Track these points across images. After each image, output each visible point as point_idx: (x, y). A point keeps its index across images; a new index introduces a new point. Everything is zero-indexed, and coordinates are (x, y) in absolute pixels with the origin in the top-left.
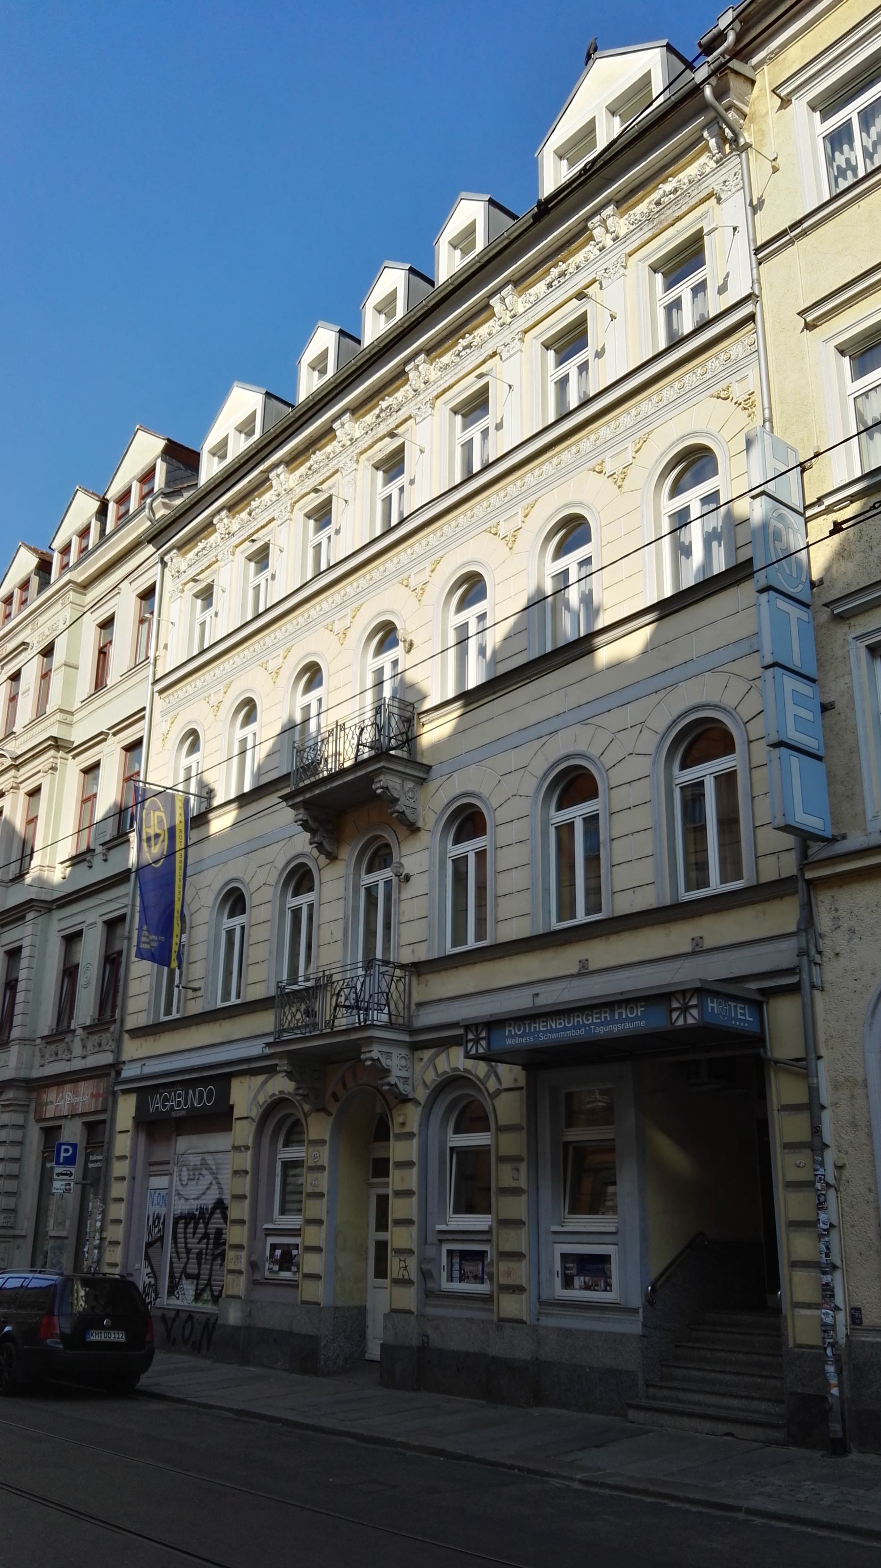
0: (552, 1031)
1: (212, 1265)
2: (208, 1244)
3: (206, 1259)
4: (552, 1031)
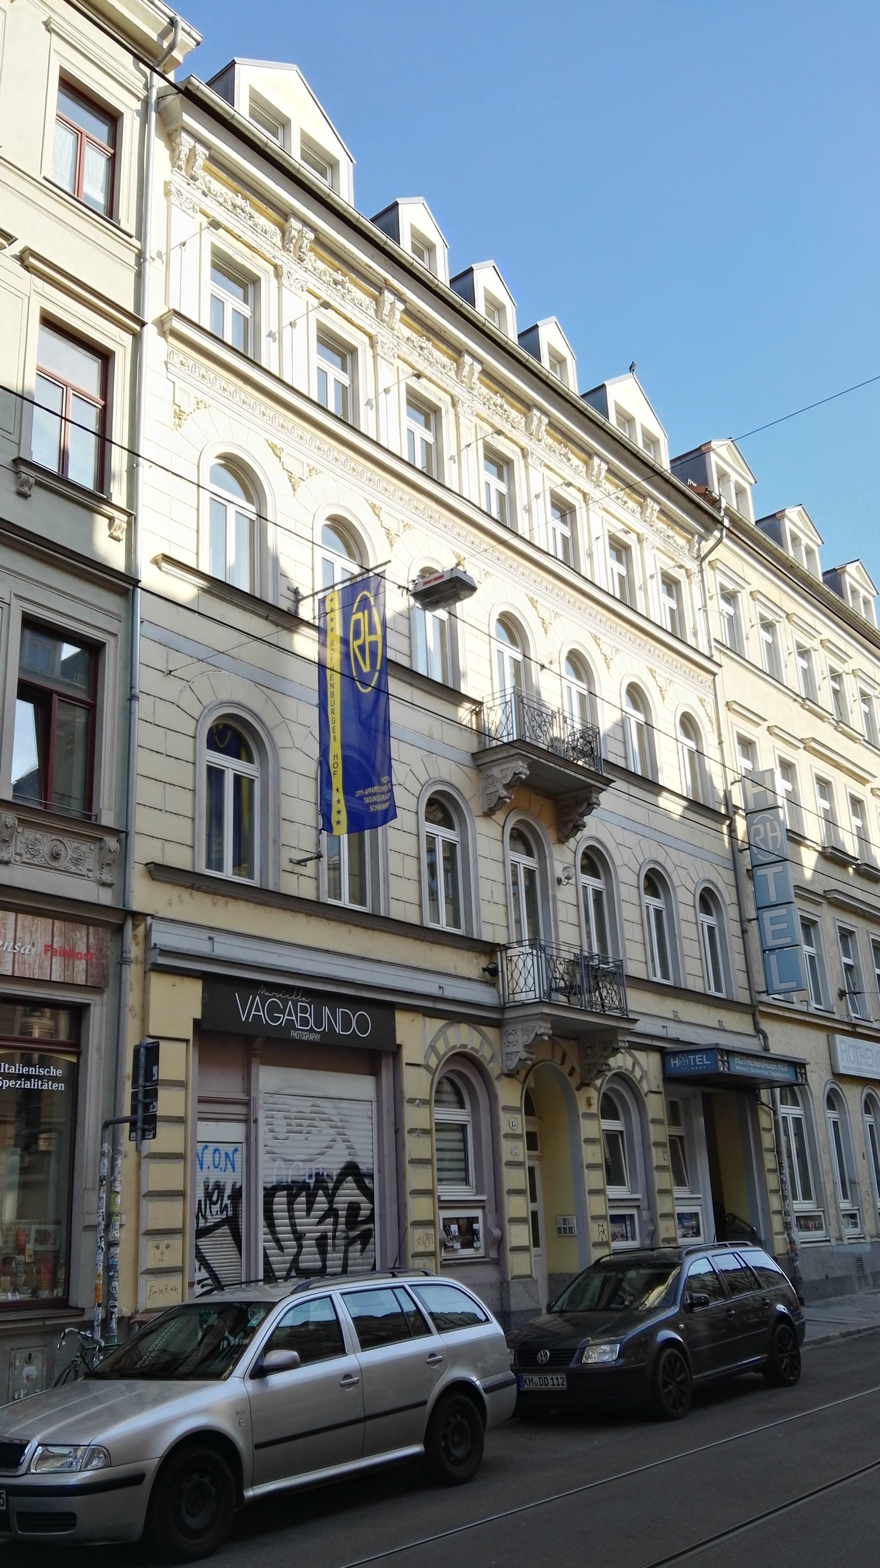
0: (754, 1067)
1: (346, 1252)
2: (336, 1223)
3: (334, 1245)
4: (754, 1067)
